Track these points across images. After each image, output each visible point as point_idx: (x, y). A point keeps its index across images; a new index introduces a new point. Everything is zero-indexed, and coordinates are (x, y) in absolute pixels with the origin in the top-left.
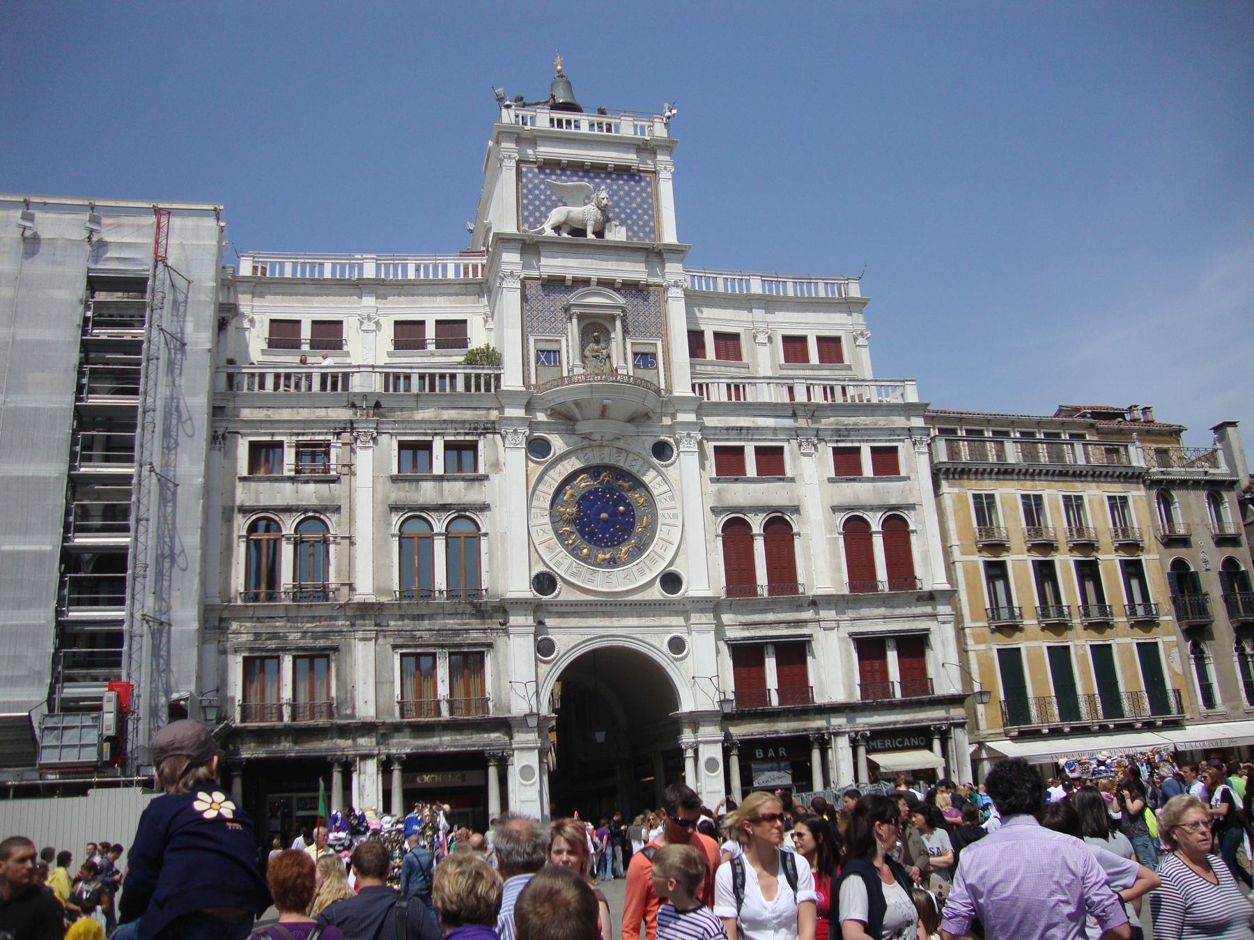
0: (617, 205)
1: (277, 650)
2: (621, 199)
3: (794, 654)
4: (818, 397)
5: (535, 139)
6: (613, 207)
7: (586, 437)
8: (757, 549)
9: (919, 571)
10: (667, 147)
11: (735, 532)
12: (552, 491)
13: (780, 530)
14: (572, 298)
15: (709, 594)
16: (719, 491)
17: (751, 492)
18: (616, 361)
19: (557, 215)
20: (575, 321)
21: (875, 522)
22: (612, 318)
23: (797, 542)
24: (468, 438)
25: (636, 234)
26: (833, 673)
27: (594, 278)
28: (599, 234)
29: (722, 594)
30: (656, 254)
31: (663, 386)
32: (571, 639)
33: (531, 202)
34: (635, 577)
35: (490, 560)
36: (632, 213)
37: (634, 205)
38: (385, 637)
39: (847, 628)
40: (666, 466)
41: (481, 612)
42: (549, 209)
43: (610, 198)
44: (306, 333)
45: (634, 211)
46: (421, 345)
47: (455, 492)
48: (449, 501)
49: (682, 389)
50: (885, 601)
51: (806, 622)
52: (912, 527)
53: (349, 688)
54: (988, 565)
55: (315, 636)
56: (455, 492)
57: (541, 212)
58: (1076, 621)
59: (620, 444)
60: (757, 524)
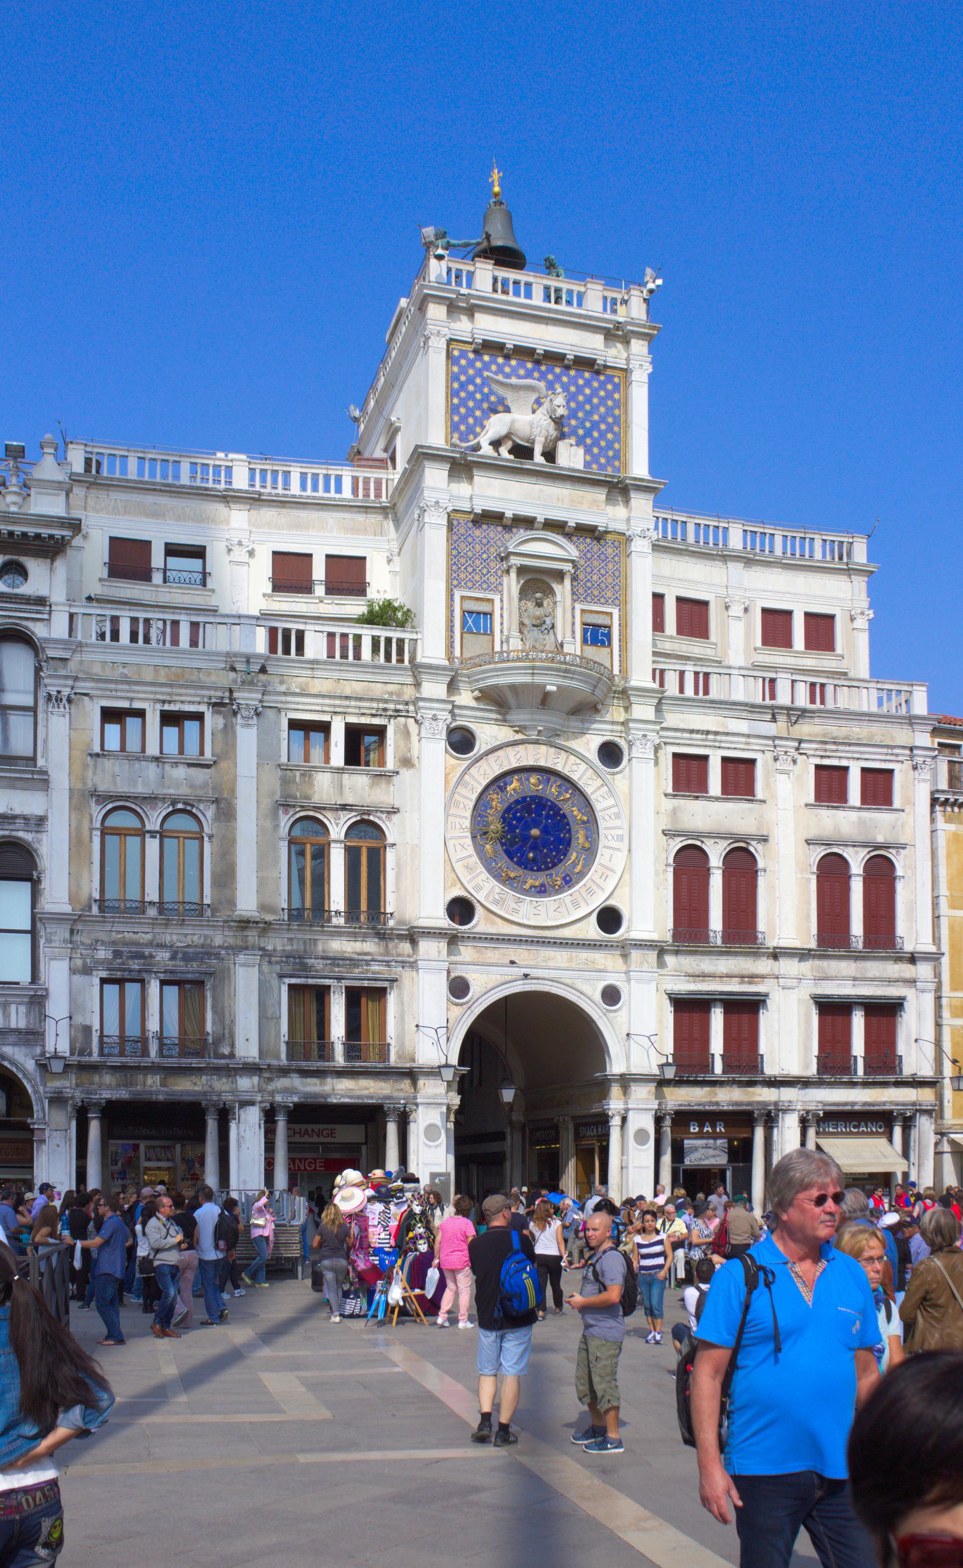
1: (140, 971)
4: (802, 700)
9: (901, 928)
12: (474, 797)
15: (655, 936)
16: (675, 811)
17: (713, 814)
18: (562, 631)
21: (857, 861)
22: (559, 575)
23: (761, 881)
24: (376, 721)
29: (669, 937)
32: (491, 982)
35: (398, 877)
38: (270, 962)
40: (613, 774)
48: (350, 802)
49: (641, 677)
51: (763, 977)
52: (899, 872)
53: (227, 1022)
55: (187, 958)
59: (560, 741)
60: (716, 854)
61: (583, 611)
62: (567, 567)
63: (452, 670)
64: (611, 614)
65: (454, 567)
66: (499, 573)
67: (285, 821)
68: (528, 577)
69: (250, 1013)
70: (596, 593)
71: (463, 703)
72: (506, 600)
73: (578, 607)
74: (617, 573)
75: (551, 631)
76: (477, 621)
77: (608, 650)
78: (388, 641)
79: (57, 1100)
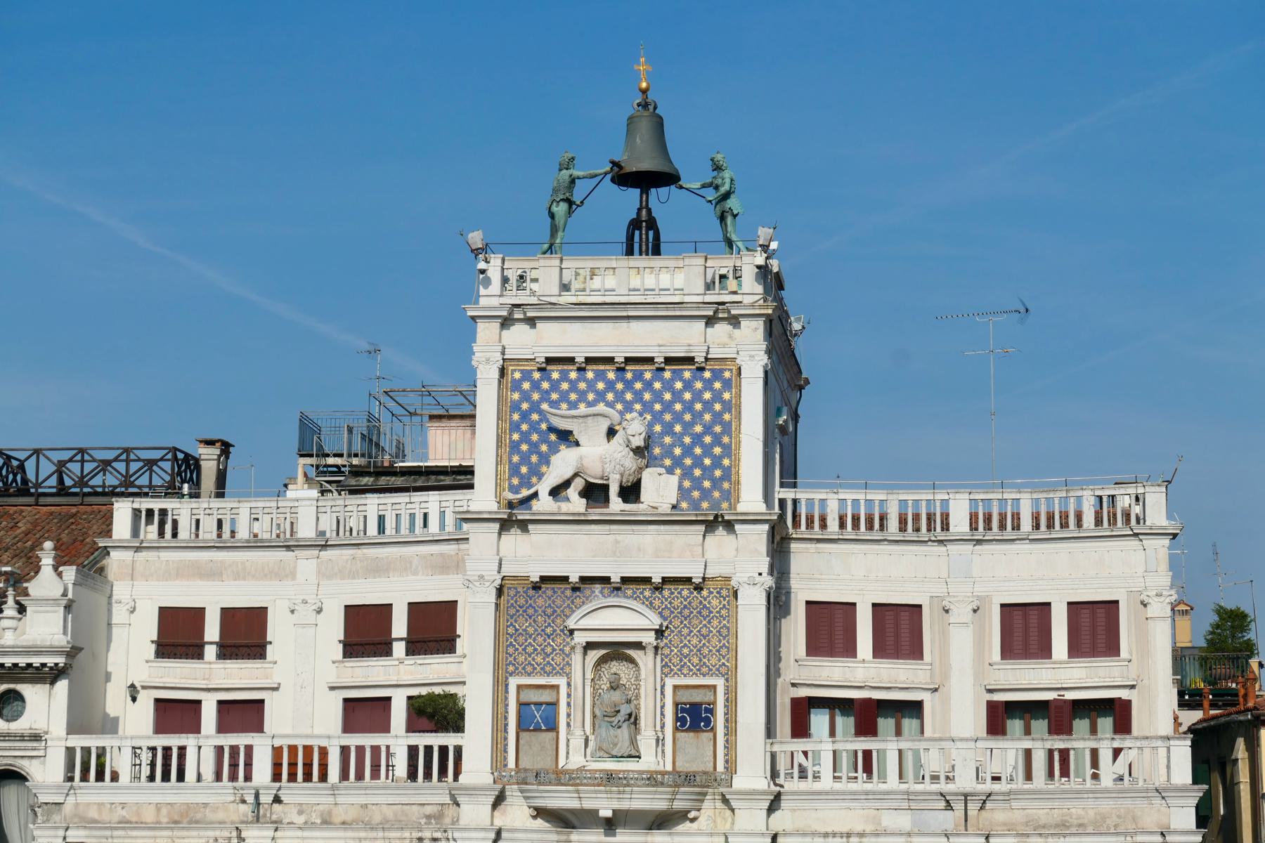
0: (668, 429)
2: (678, 417)
6: (663, 434)
19: (563, 464)
20: (577, 658)
25: (697, 484)
27: (615, 579)
28: (631, 492)
31: (720, 767)
33: (525, 437)
36: (694, 444)
37: (698, 429)
42: (554, 450)
43: (657, 417)
44: (212, 631)
45: (698, 439)
46: (382, 648)
57: (540, 454)
61: (676, 687)
62: (649, 638)
63: (493, 790)
64: (714, 687)
65: (511, 650)
66: (567, 649)
68: (603, 652)
70: (695, 660)
71: (518, 824)
72: (576, 686)
73: (670, 683)
74: (724, 632)
75: (625, 725)
76: (538, 718)
77: (711, 735)
78: (429, 749)
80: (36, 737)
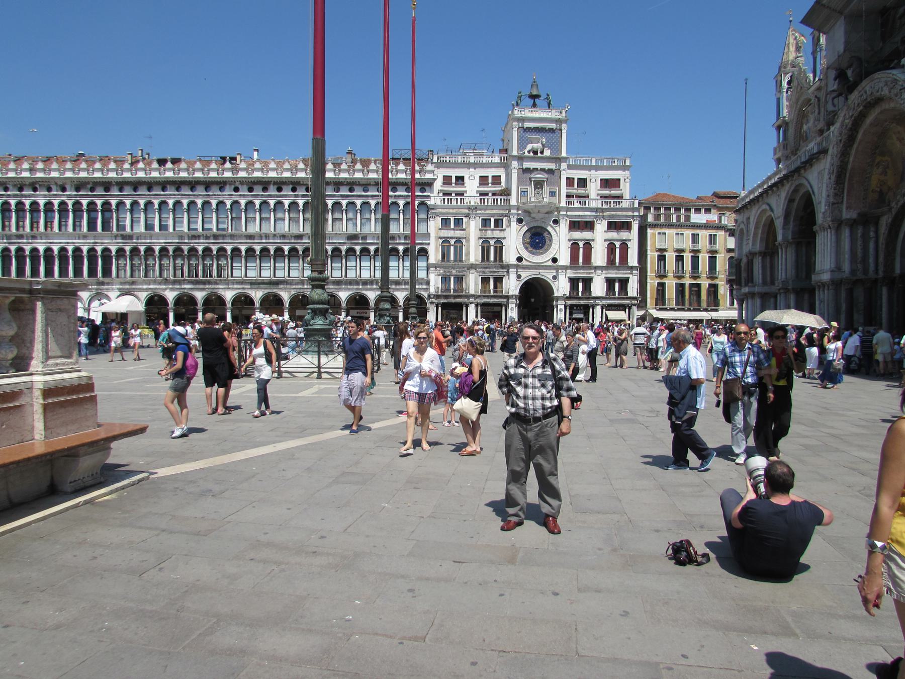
0: (547, 141)
3: (587, 282)
5: (523, 120)
7: (534, 218)
8: (581, 253)
10: (565, 121)
11: (574, 246)
13: (588, 245)
14: (532, 176)
19: (529, 147)
26: (598, 288)
28: (542, 153)
30: (558, 160)
32: (526, 275)
34: (544, 258)
39: (604, 276)
41: (502, 267)
47: (497, 234)
50: (618, 268)
54: (659, 256)
56: (497, 234)
58: (687, 275)
60: (581, 244)
67: (481, 241)
69: (473, 283)
79: (432, 303)
80: (429, 196)
